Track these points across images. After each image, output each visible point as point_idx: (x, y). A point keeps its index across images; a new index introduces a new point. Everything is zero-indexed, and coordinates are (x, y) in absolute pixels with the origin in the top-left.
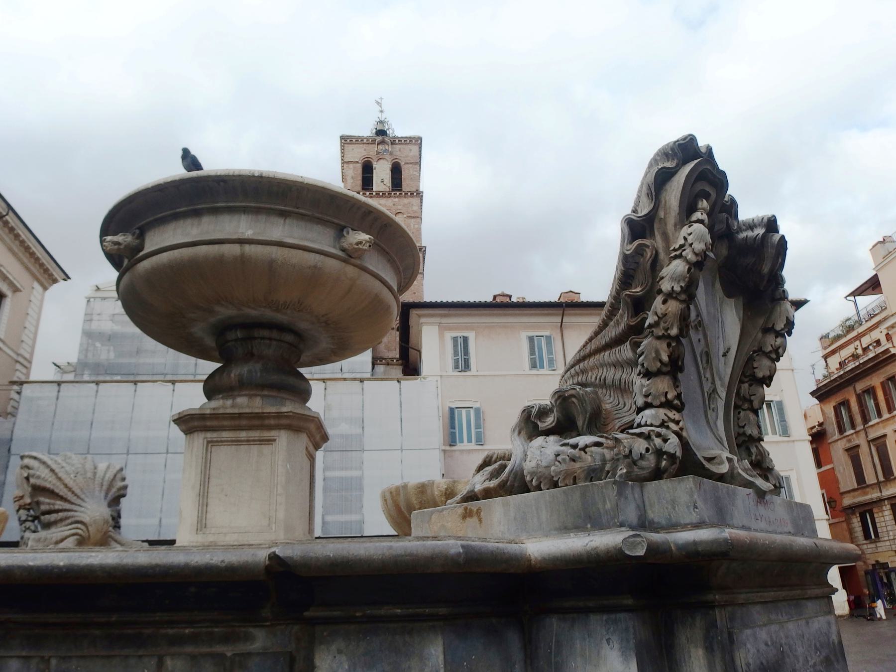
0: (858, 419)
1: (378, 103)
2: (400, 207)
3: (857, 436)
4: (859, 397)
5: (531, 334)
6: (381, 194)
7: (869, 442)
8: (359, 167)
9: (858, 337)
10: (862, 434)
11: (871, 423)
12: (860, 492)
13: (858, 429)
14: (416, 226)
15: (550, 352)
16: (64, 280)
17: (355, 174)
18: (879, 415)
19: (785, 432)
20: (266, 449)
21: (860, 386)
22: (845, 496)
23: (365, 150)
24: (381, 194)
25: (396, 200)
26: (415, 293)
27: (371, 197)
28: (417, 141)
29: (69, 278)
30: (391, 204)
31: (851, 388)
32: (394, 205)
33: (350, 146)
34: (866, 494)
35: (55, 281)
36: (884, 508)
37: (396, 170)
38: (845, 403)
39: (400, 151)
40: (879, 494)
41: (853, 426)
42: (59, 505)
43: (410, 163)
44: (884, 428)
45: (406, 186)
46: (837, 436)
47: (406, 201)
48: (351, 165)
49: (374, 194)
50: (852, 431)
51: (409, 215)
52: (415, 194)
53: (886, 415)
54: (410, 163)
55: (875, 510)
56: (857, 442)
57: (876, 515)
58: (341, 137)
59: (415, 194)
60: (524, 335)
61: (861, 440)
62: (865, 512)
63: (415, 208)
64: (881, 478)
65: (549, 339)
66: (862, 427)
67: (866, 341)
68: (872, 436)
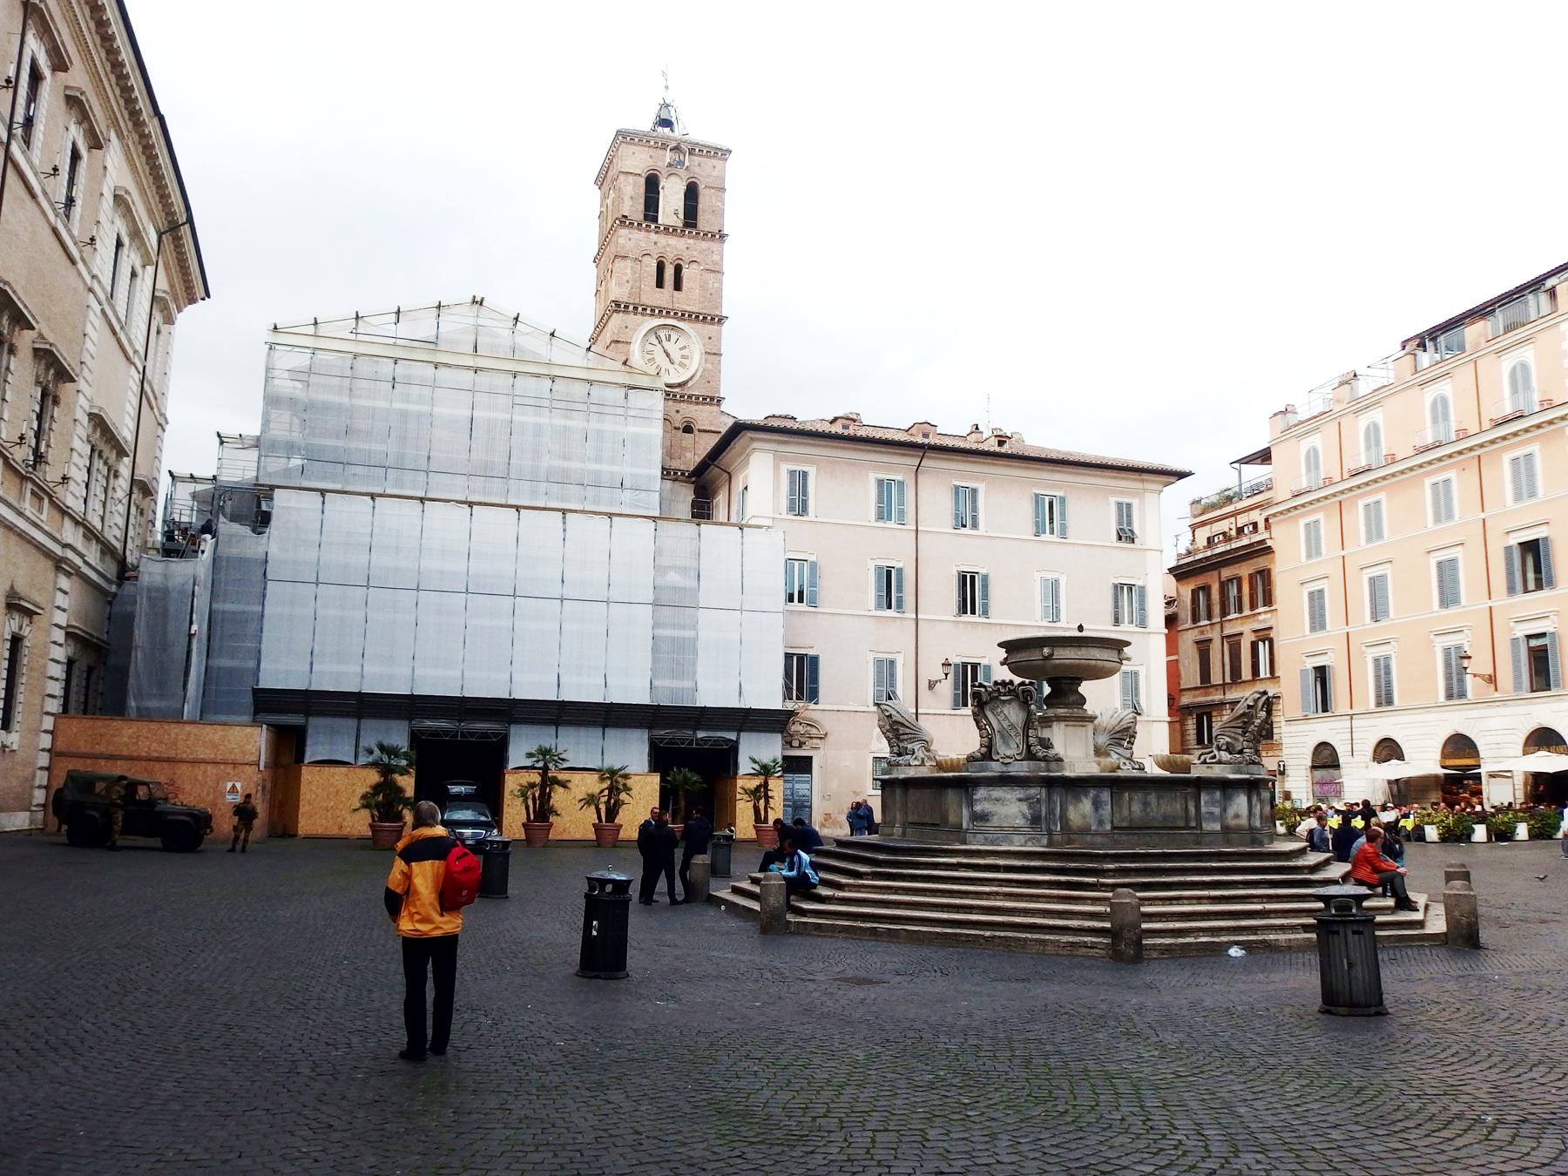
0: (1216, 609)
2: (695, 253)
3: (1212, 629)
4: (1224, 587)
5: (882, 476)
6: (671, 230)
7: (1223, 637)
8: (642, 181)
9: (1235, 514)
10: (1218, 628)
11: (1229, 618)
12: (1202, 690)
13: (1214, 621)
14: (716, 285)
15: (901, 502)
16: (203, 299)
17: (636, 193)
18: (1240, 610)
19: (1143, 623)
20: (1084, 729)
21: (1226, 573)
22: (1184, 693)
23: (651, 157)
24: (671, 230)
25: (691, 241)
26: (709, 382)
27: (657, 233)
28: (721, 154)
29: (209, 297)
30: (684, 247)
31: (1215, 573)
32: (687, 248)
33: (630, 147)
34: (1207, 694)
35: (192, 300)
36: (1224, 712)
37: (692, 193)
38: (1206, 589)
39: (699, 165)
40: (1222, 697)
41: (1209, 617)
42: (907, 731)
43: (713, 188)
44: (1242, 624)
45: (704, 221)
46: (1189, 624)
47: (704, 245)
48: (631, 179)
49: (662, 228)
50: (1207, 622)
51: (708, 267)
52: (718, 236)
53: (1247, 612)
54: (713, 188)
55: (1214, 713)
56: (1209, 636)
57: (1214, 719)
58: (618, 133)
59: (718, 236)
60: (873, 477)
61: (1215, 635)
62: (1203, 714)
63: (716, 258)
64: (1228, 680)
65: (901, 484)
66: (1219, 620)
67: (1242, 520)
68: (1227, 632)
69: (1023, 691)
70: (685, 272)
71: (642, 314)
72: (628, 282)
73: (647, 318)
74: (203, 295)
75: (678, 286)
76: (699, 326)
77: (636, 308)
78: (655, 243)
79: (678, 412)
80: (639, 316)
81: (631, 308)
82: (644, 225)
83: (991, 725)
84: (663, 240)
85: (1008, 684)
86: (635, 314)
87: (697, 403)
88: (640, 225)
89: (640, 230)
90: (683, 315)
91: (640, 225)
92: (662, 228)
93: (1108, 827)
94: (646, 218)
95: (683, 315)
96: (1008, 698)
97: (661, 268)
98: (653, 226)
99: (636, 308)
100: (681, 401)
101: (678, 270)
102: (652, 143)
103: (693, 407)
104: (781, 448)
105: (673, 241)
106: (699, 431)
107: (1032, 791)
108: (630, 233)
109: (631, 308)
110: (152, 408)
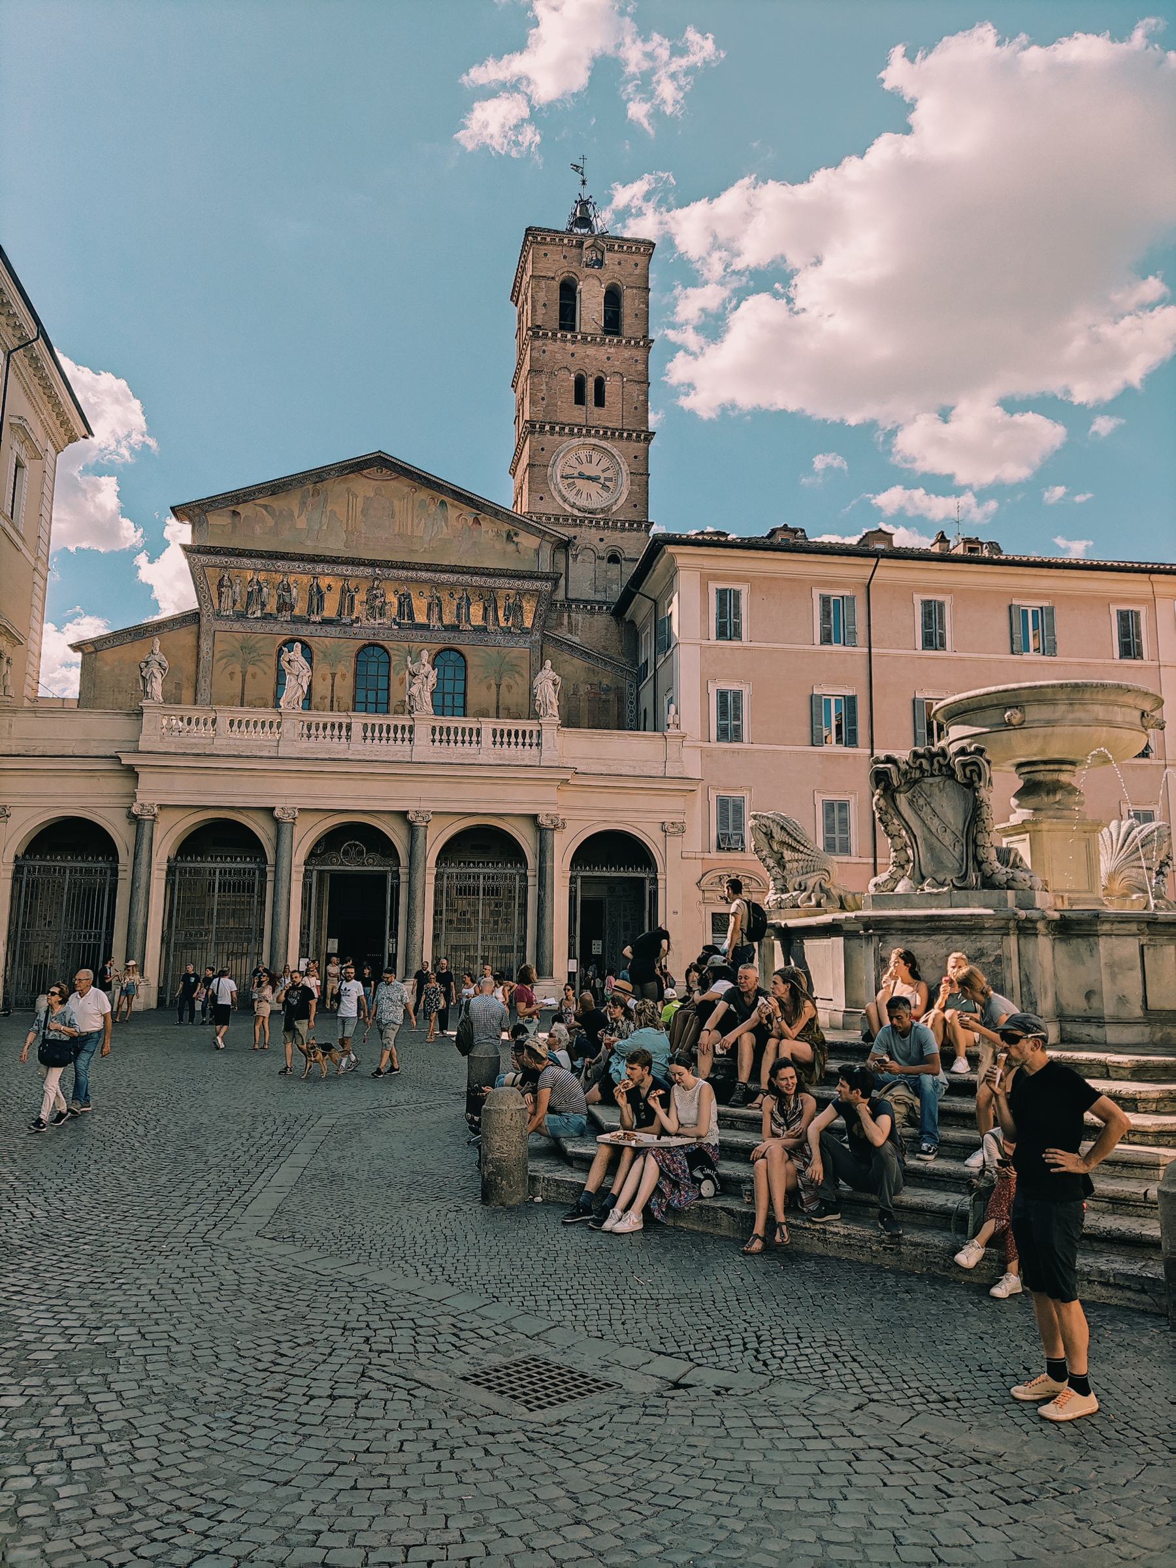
1: (576, 168)
16: (85, 437)
23: (565, 257)
27: (573, 343)
29: (93, 435)
32: (608, 358)
35: (73, 439)
37: (613, 297)
39: (619, 264)
49: (579, 337)
58: (529, 230)
69: (964, 765)
70: (608, 384)
71: (560, 434)
72: (543, 399)
73: (565, 438)
74: (84, 431)
75: (600, 401)
76: (624, 444)
77: (552, 428)
78: (573, 355)
79: (602, 540)
80: (556, 437)
81: (547, 428)
82: (559, 335)
83: (909, 829)
84: (580, 350)
85: (937, 755)
86: (552, 434)
87: (623, 529)
88: (555, 335)
89: (555, 341)
90: (605, 433)
91: (555, 335)
92: (579, 337)
93: (1138, 1012)
94: (562, 327)
95: (605, 433)
96: (937, 779)
97: (580, 383)
98: (569, 336)
99: (552, 428)
100: (604, 529)
101: (599, 384)
102: (566, 241)
103: (618, 535)
104: (707, 563)
105: (591, 351)
106: (625, 559)
107: (986, 942)
108: (544, 344)
109: (547, 428)
110: (19, 550)
